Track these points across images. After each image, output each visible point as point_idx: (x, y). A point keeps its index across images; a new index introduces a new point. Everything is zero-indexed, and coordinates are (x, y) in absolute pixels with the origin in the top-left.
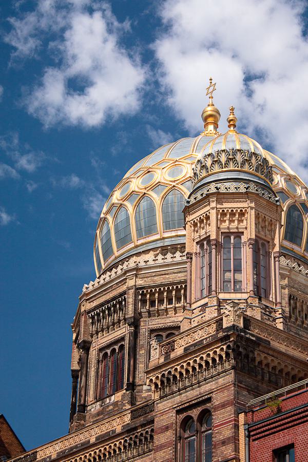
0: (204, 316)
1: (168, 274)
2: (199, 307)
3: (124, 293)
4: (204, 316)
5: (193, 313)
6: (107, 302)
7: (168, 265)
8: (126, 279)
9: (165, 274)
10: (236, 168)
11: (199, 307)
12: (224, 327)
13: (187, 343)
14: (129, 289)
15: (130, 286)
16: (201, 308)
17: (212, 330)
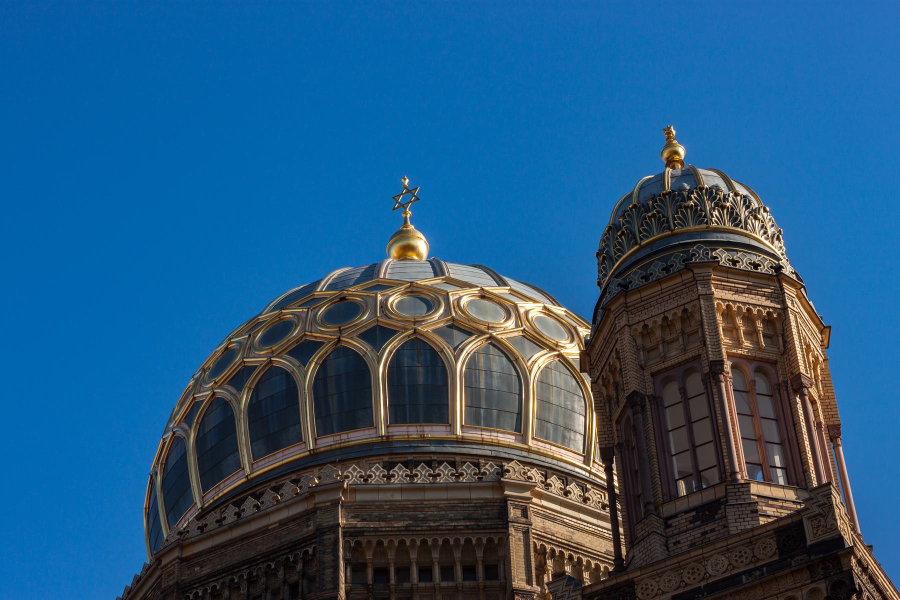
0: (713, 530)
1: (422, 510)
2: (686, 512)
3: (307, 540)
4: (713, 530)
5: (670, 526)
6: (250, 562)
7: (422, 489)
8: (314, 511)
9: (415, 509)
10: (739, 229)
11: (686, 512)
12: (809, 543)
13: (703, 579)
14: (323, 533)
15: (325, 524)
16: (694, 513)
17: (768, 552)
